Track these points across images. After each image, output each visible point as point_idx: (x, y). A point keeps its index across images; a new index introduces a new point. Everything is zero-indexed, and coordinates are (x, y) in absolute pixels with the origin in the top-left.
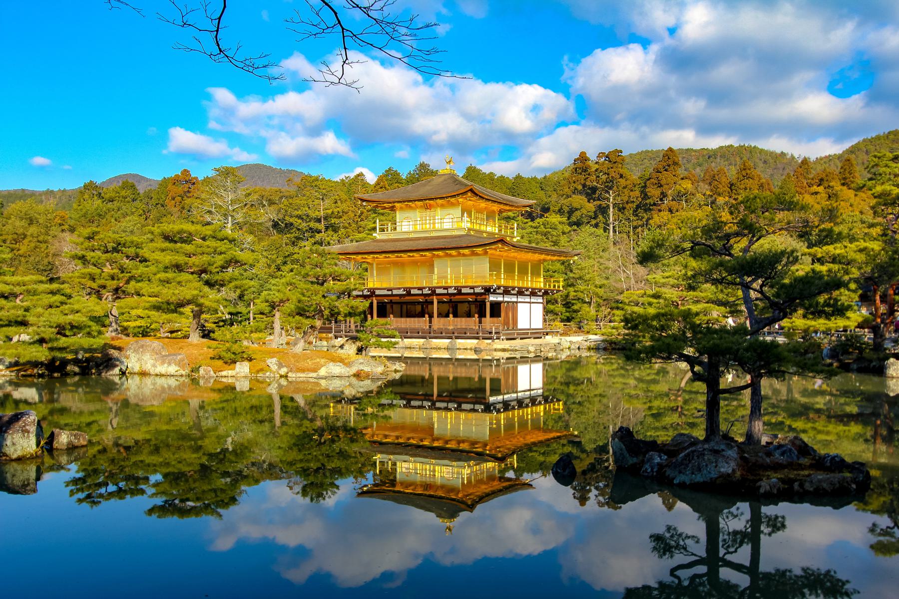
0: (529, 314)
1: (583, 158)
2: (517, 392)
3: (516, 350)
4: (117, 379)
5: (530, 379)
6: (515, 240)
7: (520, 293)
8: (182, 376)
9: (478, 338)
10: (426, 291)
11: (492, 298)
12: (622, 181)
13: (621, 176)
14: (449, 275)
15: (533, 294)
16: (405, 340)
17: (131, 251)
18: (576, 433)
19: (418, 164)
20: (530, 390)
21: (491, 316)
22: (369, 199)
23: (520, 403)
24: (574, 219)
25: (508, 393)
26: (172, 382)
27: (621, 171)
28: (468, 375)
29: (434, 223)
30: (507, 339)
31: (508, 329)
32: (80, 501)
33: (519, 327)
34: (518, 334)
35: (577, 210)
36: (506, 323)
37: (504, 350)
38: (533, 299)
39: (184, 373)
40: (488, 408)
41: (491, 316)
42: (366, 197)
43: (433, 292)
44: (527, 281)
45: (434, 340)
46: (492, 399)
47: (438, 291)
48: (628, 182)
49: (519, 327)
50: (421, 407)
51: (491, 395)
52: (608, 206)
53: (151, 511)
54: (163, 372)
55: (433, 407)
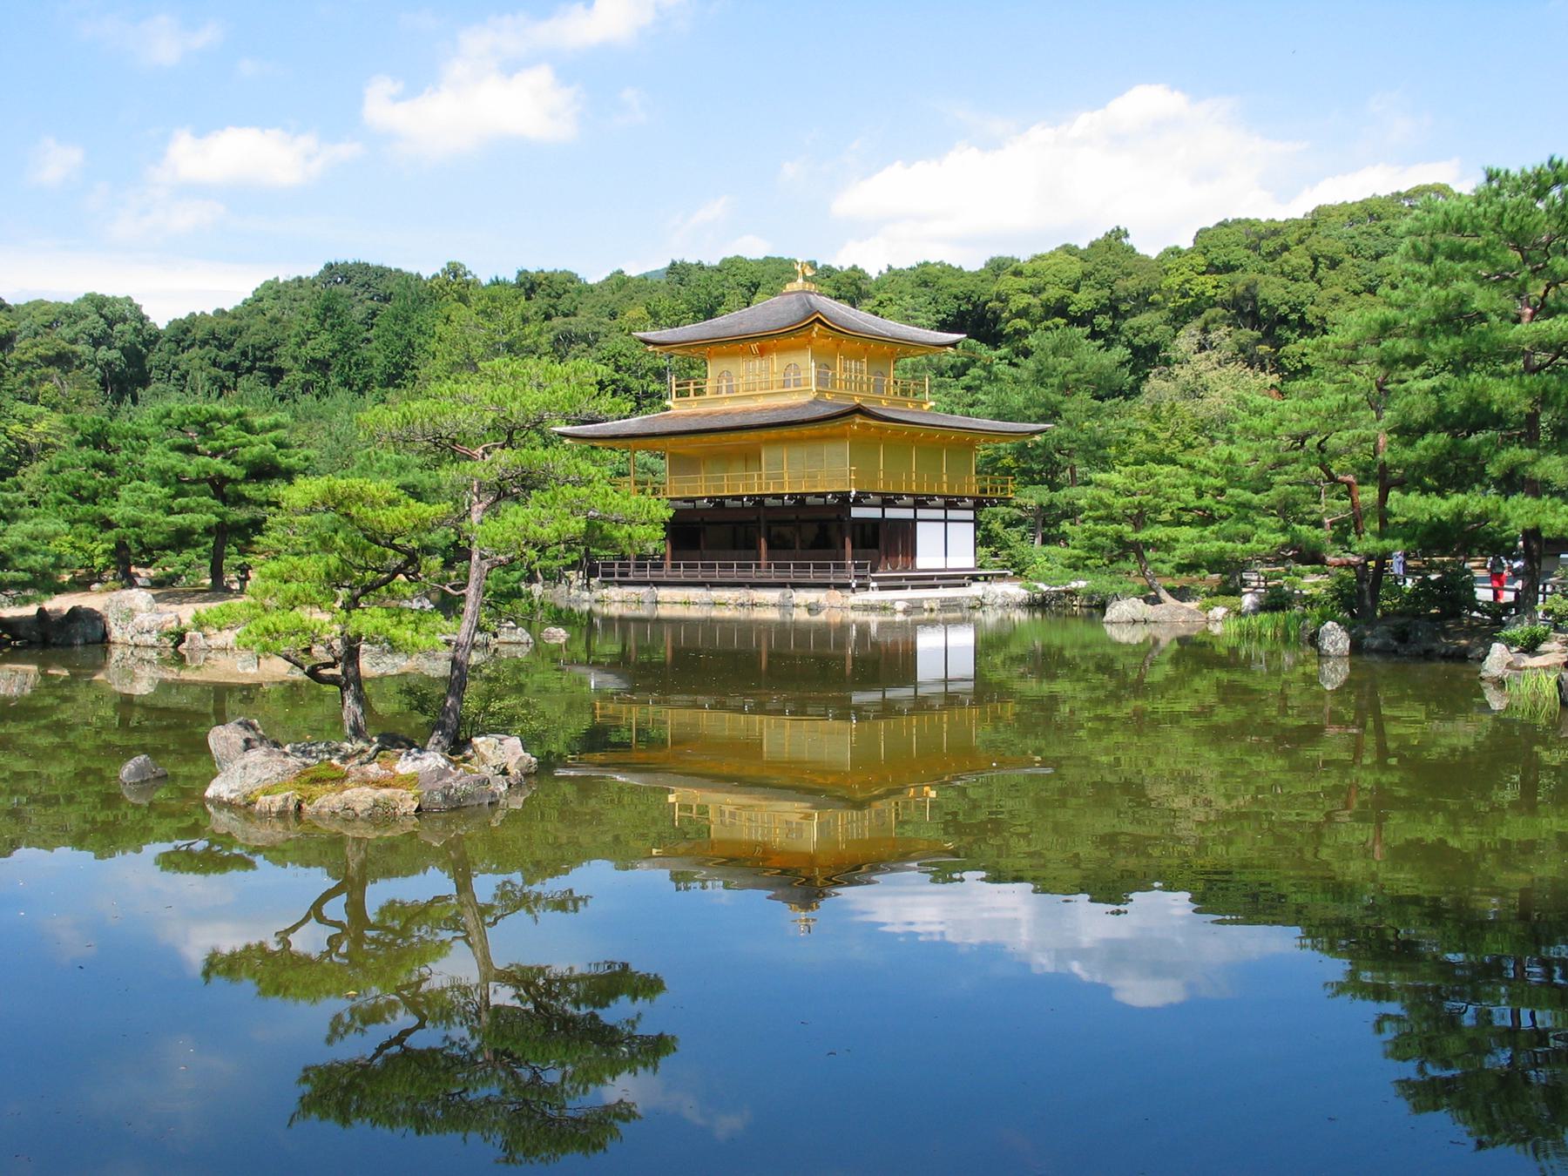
3: (885, 608)
6: (926, 407)
7: (920, 502)
9: (826, 586)
11: (856, 512)
14: (787, 475)
15: (950, 504)
20: (946, 681)
23: (921, 705)
30: (881, 588)
34: (908, 579)
38: (952, 514)
40: (845, 711)
46: (858, 698)
47: (769, 502)
50: (741, 710)
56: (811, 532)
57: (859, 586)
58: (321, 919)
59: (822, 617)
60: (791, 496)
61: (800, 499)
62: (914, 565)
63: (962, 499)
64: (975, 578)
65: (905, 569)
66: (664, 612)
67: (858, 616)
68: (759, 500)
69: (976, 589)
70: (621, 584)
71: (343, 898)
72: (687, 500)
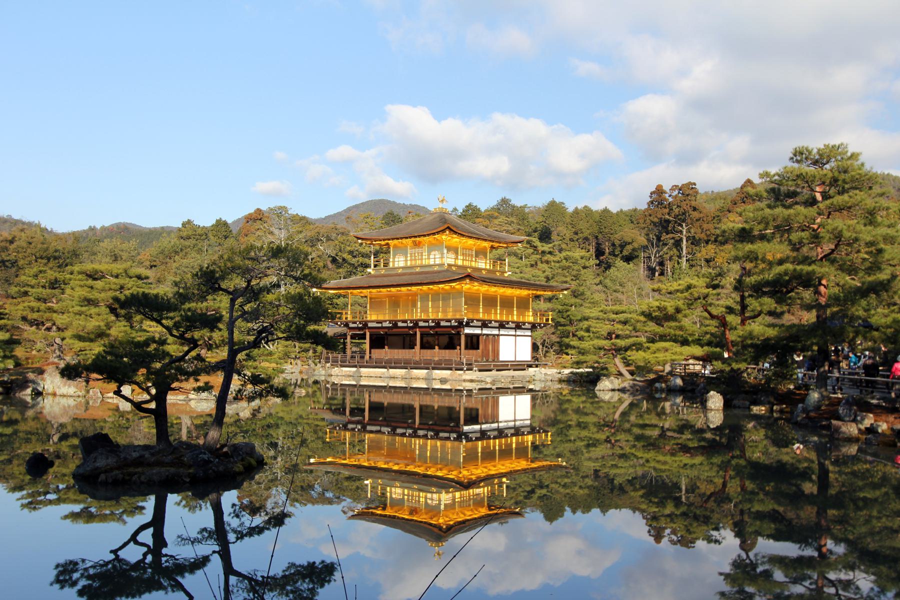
0: (515, 347)
1: (659, 191)
2: (498, 422)
4: (29, 399)
5: (514, 410)
6: (506, 275)
7: (502, 325)
8: (79, 396)
9: (451, 369)
10: (454, 323)
11: (468, 331)
12: (695, 215)
13: (695, 209)
15: (518, 326)
16: (391, 370)
17: (237, 282)
18: (564, 464)
19: (499, 199)
20: (515, 421)
21: (466, 348)
22: (363, 237)
24: (625, 253)
25: (486, 423)
26: (71, 402)
27: (693, 204)
28: (451, 405)
29: (422, 259)
30: (480, 371)
31: (487, 361)
32: (23, 506)
33: (501, 359)
34: (494, 366)
35: (629, 243)
36: (486, 354)
37: (472, 381)
38: (519, 332)
39: (81, 394)
41: (466, 348)
42: (360, 234)
43: (365, 325)
44: (496, 314)
45: (415, 371)
46: (466, 428)
47: (421, 324)
48: (702, 215)
49: (501, 359)
51: (466, 424)
52: (681, 240)
53: (66, 517)
54: (65, 393)
55: (415, 435)
56: (445, 340)
57: (468, 370)
58: (137, 543)
59: (447, 386)
60: (433, 321)
61: (438, 323)
62: (498, 358)
63: (524, 324)
64: (530, 366)
65: (494, 361)
66: (363, 382)
67: (469, 386)
68: (416, 324)
69: (531, 370)
70: (342, 366)
71: (151, 530)
72: (378, 322)
